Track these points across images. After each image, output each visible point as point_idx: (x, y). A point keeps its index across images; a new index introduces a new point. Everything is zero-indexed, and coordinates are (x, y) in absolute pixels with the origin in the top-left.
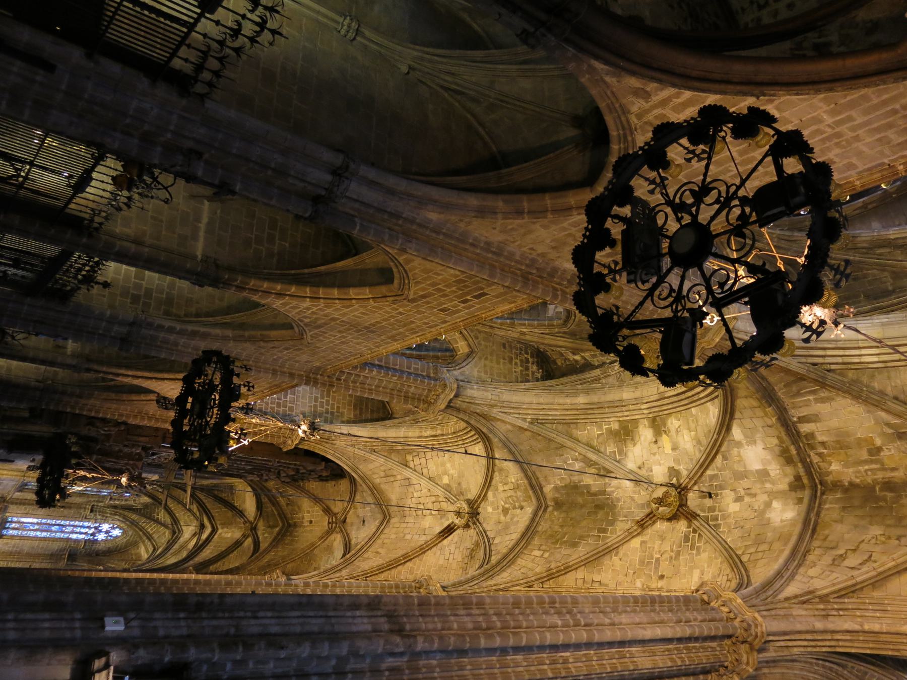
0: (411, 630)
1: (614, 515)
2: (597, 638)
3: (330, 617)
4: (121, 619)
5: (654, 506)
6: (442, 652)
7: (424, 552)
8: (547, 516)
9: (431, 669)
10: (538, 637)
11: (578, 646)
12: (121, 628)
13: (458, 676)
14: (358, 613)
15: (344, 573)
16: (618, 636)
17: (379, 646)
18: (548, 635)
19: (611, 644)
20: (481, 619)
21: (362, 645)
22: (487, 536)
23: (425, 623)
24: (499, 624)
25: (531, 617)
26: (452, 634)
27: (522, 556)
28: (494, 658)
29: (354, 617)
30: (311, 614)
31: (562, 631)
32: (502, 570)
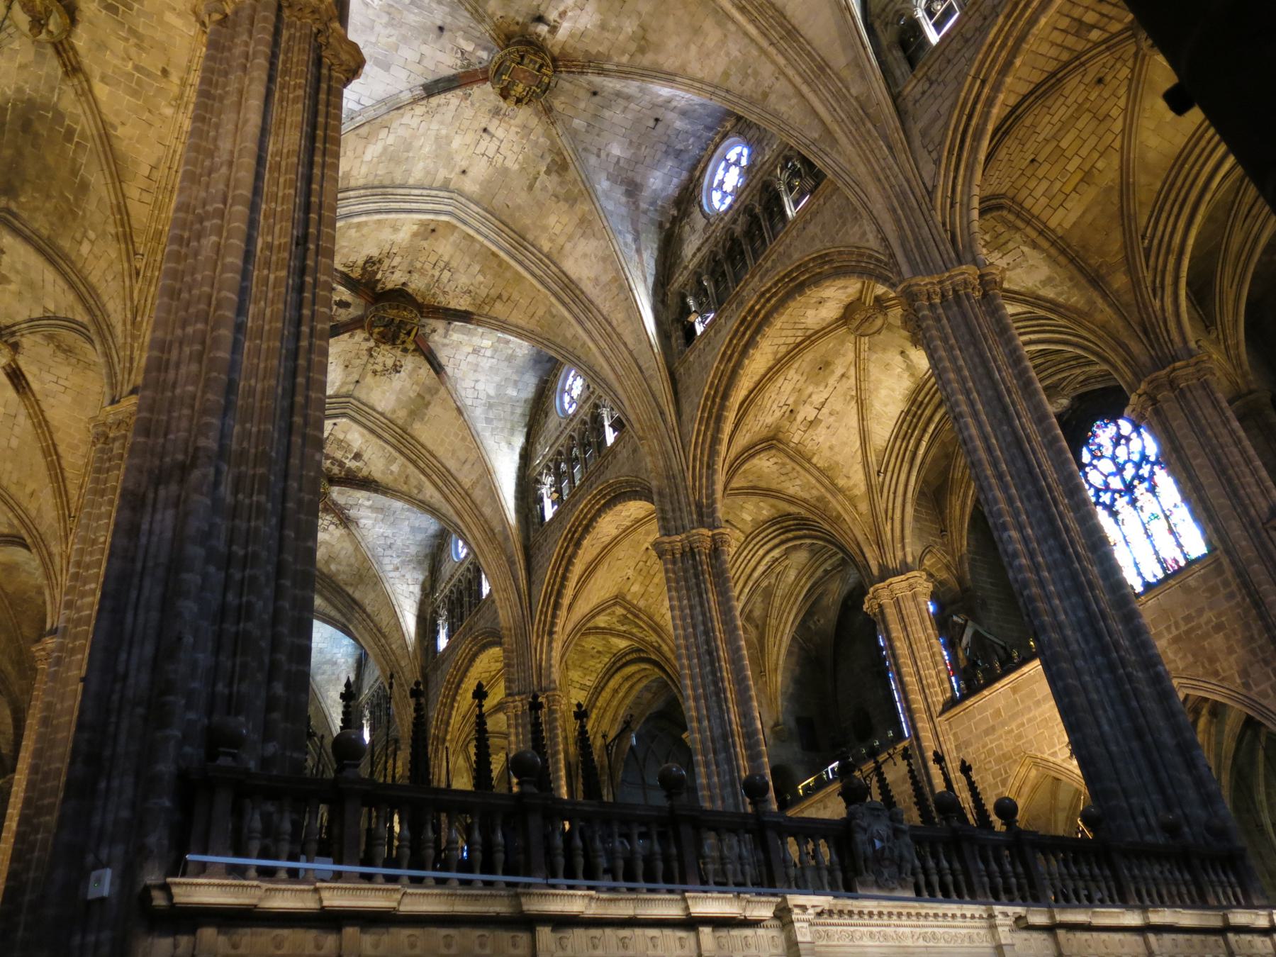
0: (186, 452)
1: (46, 107)
2: (246, 192)
3: (144, 568)
4: (94, 874)
5: (43, 36)
6: (225, 415)
7: (46, 422)
8: (25, 215)
9: (246, 435)
10: (230, 275)
11: (252, 224)
12: (108, 874)
13: (262, 401)
14: (145, 527)
15: (56, 549)
16: (249, 161)
17: (201, 501)
18: (229, 260)
19: (258, 177)
20: (187, 350)
21: (195, 525)
22: (39, 319)
23: (178, 431)
24: (200, 326)
25: (199, 277)
26: (202, 396)
27: (86, 272)
28: (247, 344)
29: (151, 532)
30: (134, 594)
31: (228, 238)
32: (102, 308)
